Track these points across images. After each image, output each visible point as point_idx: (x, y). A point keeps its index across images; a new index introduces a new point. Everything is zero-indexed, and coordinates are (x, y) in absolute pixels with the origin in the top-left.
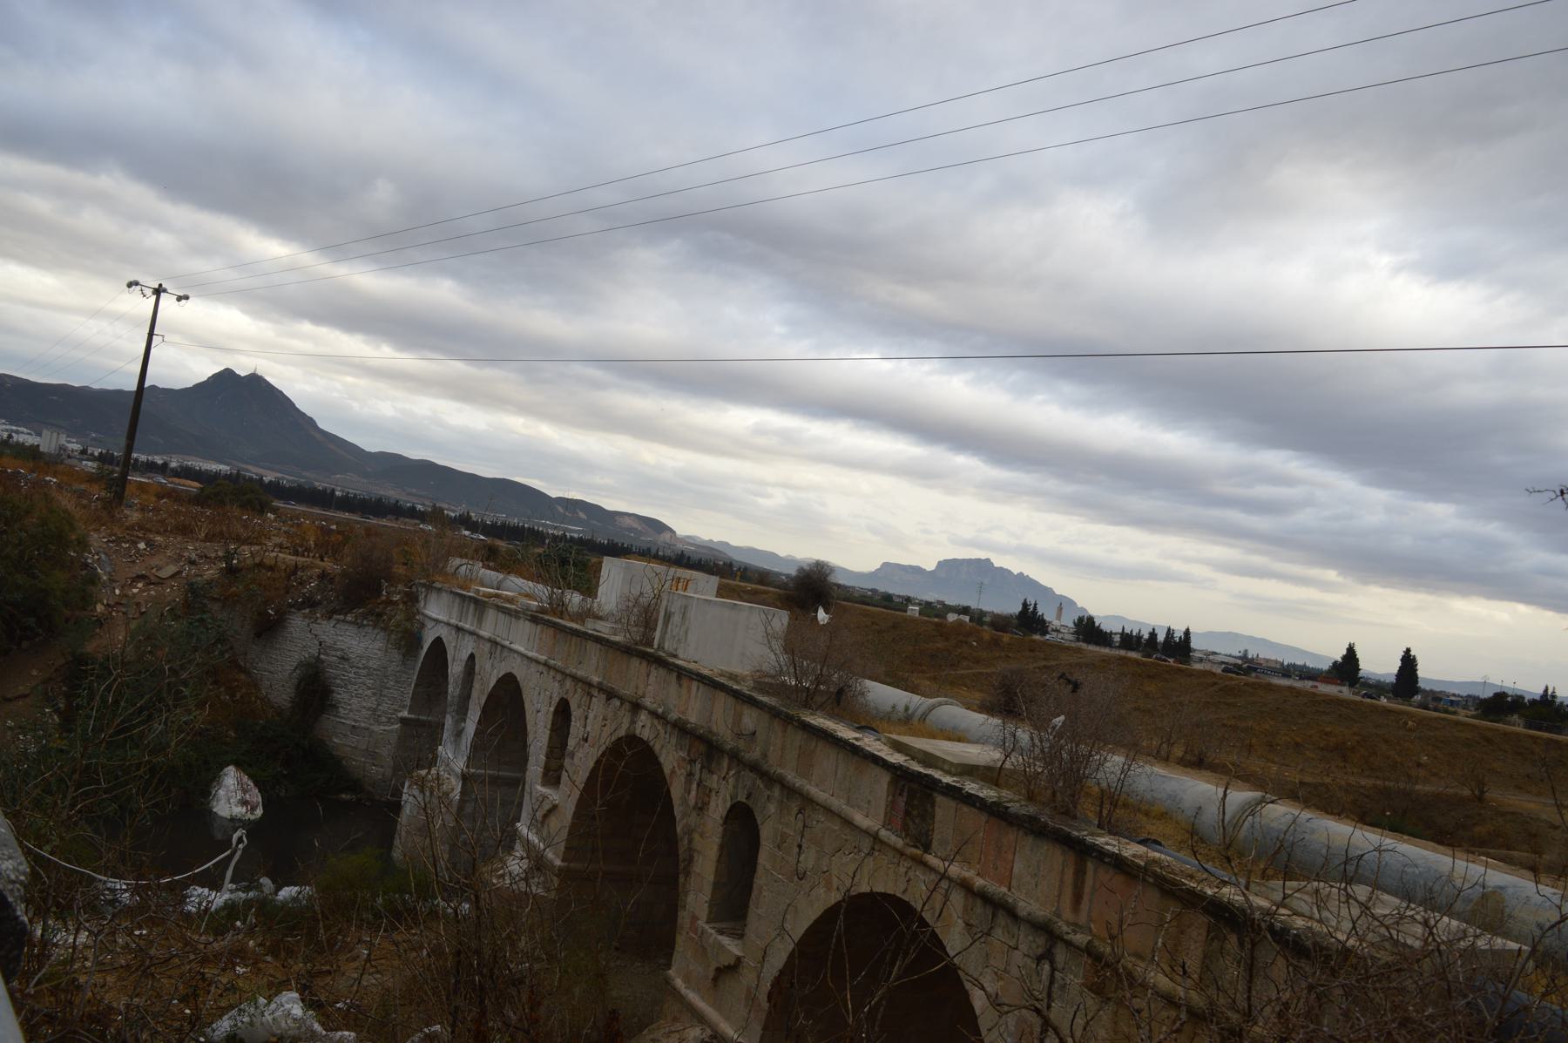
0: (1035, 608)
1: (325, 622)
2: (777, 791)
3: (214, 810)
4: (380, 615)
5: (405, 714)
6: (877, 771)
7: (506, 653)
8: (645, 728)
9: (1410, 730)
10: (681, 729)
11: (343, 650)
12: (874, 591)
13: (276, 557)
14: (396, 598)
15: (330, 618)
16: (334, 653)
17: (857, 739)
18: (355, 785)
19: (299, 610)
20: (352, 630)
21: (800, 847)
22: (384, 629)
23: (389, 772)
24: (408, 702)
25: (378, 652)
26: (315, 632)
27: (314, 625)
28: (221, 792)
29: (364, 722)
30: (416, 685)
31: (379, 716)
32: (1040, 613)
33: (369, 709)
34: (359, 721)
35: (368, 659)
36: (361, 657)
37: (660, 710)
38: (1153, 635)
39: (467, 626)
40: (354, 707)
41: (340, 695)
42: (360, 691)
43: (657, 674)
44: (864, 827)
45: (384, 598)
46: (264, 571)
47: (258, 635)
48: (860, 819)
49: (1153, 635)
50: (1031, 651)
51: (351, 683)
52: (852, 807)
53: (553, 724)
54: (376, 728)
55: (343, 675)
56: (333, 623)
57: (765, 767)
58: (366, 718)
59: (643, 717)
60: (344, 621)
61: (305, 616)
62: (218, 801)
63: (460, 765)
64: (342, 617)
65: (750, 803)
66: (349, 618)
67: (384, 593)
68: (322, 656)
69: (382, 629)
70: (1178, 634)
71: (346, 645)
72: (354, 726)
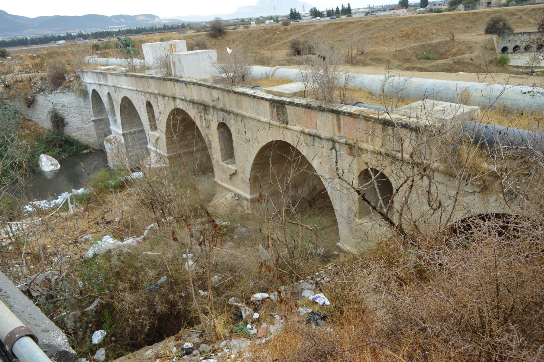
0: (295, 10)
2: (232, 116)
3: (44, 170)
4: (69, 87)
5: (93, 118)
6: (264, 102)
7: (120, 90)
8: (180, 105)
9: (429, 22)
10: (193, 102)
12: (237, 19)
13: (21, 77)
14: (72, 79)
15: (52, 93)
17: (254, 93)
18: (87, 147)
19: (39, 93)
20: (61, 95)
21: (245, 132)
22: (73, 91)
23: (96, 139)
24: (93, 114)
28: (43, 164)
30: (93, 108)
32: (297, 12)
33: (80, 120)
35: (72, 103)
37: (183, 98)
38: (337, 9)
39: (102, 83)
40: (75, 121)
41: (67, 119)
42: (74, 115)
43: (177, 85)
44: (265, 121)
45: (68, 80)
46: (19, 83)
47: (29, 107)
48: (262, 119)
49: (337, 9)
50: (299, 30)
52: (259, 115)
53: (147, 110)
54: (85, 126)
56: (53, 95)
57: (226, 109)
59: (178, 101)
60: (57, 93)
61: (42, 95)
62: (43, 167)
63: (121, 132)
64: (56, 92)
65: (224, 122)
66: (58, 91)
67: (67, 78)
68: (55, 107)
69: (72, 91)
70: (346, 6)
72: (77, 128)
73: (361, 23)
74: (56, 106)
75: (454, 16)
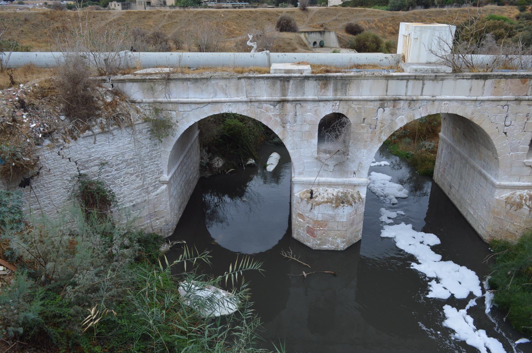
1: (71, 144)
9: (223, 18)
11: (99, 158)
16: (92, 164)
25: (129, 146)
26: (68, 157)
27: (65, 150)
29: (138, 198)
31: (148, 188)
33: (138, 188)
34: (133, 200)
35: (123, 154)
36: (117, 155)
40: (126, 193)
42: (127, 180)
51: (116, 178)
55: (108, 176)
58: (137, 195)
61: (51, 148)
68: (82, 172)
71: (101, 153)
72: (134, 206)
73: (162, 14)
74: (86, 168)
75: (238, 13)
